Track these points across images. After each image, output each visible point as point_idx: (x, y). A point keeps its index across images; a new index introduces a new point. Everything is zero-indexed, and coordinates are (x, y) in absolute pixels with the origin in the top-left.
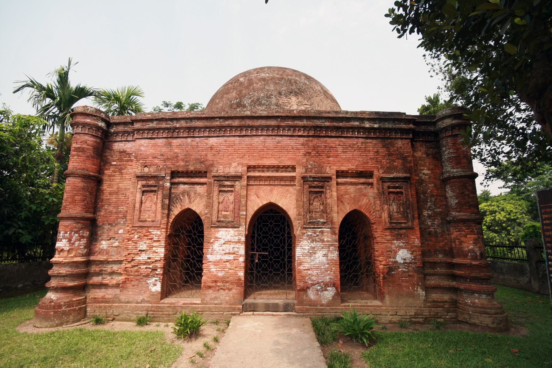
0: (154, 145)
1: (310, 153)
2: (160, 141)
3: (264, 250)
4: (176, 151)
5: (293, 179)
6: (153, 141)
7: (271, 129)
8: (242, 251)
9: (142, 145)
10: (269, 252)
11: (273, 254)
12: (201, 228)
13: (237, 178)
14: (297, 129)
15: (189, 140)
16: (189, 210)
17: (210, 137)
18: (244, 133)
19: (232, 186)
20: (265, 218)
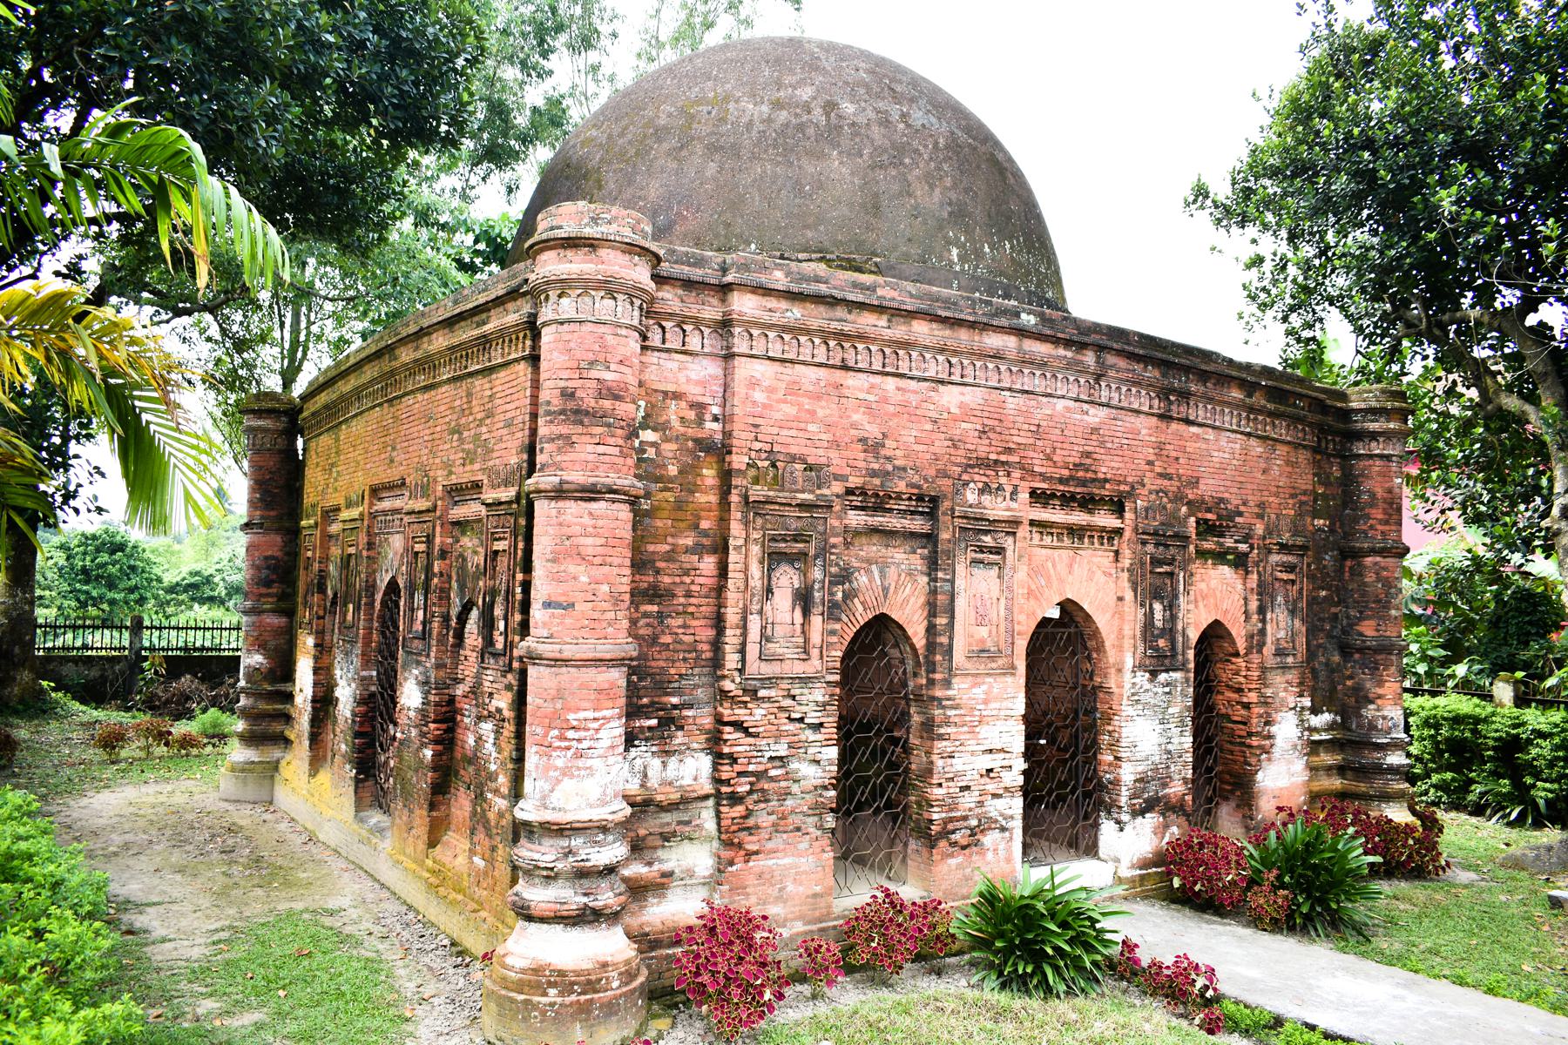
4: (856, 417)
5: (1118, 532)
6: (788, 370)
8: (1018, 744)
9: (753, 384)
15: (891, 383)
16: (883, 615)
17: (942, 382)
18: (1026, 382)
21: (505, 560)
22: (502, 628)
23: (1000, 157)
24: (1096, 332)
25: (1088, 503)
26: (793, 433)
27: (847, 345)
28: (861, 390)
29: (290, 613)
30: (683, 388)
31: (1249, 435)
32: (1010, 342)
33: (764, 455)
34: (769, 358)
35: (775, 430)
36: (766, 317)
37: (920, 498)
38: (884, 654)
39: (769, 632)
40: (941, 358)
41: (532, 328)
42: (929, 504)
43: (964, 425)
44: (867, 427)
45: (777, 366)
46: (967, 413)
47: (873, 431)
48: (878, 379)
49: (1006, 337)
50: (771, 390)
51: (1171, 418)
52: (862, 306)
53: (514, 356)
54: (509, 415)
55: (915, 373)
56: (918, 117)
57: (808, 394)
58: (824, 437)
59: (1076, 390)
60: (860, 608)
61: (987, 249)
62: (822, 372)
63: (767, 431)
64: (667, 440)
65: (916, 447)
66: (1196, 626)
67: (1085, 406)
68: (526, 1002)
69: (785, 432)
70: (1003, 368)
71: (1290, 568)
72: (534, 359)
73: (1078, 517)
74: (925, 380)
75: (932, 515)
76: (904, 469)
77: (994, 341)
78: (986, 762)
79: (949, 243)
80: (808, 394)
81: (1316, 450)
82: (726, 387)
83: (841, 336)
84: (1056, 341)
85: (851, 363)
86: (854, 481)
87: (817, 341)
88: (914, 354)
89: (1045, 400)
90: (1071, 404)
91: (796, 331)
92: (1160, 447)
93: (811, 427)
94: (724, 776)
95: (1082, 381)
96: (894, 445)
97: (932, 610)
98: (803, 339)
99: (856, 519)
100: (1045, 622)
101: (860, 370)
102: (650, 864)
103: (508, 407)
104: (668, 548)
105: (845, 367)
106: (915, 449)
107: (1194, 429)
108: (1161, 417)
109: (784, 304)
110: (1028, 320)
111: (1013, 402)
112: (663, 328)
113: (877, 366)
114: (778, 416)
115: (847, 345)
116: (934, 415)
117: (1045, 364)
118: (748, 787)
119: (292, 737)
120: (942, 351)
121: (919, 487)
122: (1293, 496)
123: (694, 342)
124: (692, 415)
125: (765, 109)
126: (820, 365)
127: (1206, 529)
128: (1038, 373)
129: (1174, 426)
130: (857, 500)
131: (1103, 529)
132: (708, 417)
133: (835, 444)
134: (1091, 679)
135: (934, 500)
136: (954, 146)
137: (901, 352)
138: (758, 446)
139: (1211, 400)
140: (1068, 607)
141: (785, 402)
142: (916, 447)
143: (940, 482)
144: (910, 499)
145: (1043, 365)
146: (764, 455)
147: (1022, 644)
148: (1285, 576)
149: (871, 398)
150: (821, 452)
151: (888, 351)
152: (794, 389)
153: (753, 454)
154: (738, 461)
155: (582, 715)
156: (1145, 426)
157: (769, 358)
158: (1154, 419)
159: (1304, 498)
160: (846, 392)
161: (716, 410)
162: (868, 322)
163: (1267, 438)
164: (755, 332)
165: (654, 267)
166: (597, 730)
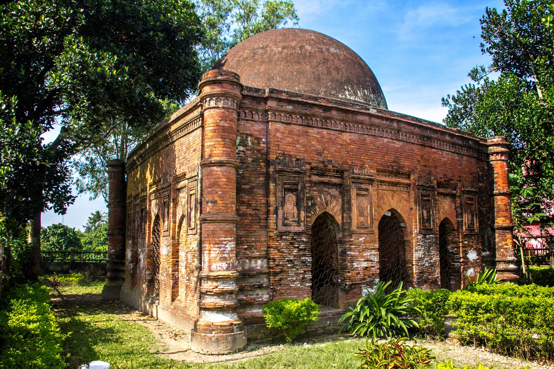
2: (297, 128)
4: (313, 143)
8: (376, 259)
9: (277, 130)
15: (325, 132)
19: (367, 190)
21: (194, 197)
22: (194, 221)
23: (362, 63)
24: (397, 116)
25: (397, 174)
26: (291, 148)
27: (309, 118)
28: (314, 134)
29: (124, 235)
30: (253, 132)
31: (453, 152)
32: (366, 118)
33: (281, 155)
34: (282, 122)
35: (285, 147)
36: (280, 108)
37: (337, 171)
38: (327, 227)
39: (285, 216)
40: (342, 123)
41: (202, 115)
42: (340, 173)
43: (351, 146)
44: (318, 146)
45: (285, 125)
46: (353, 142)
47: (319, 147)
48: (320, 130)
50: (283, 133)
51: (425, 146)
52: (314, 105)
53: (196, 127)
54: (194, 148)
55: (333, 128)
56: (332, 50)
57: (296, 135)
58: (302, 149)
59: (391, 135)
60: (318, 209)
62: (301, 128)
63: (282, 147)
64: (247, 150)
65: (335, 153)
66: (439, 219)
67: (395, 141)
68: (205, 336)
69: (289, 147)
70: (364, 127)
71: (471, 199)
72: (203, 127)
73: (394, 179)
74: (337, 131)
75: (342, 177)
76: (331, 161)
77: (360, 118)
78: (365, 264)
79: (345, 90)
80: (296, 135)
81: (478, 159)
82: (267, 132)
83: (306, 115)
84: (382, 118)
85: (311, 124)
86: (314, 165)
87: (298, 117)
88: (333, 122)
89: (380, 138)
90: (390, 140)
91: (291, 113)
92: (422, 156)
93: (298, 146)
94: (271, 266)
95: (393, 132)
96: (327, 152)
97: (343, 210)
98: (293, 116)
99: (315, 178)
100: (384, 217)
101: (314, 127)
102: (246, 296)
103: (194, 145)
104: (249, 187)
105: (309, 126)
106: (334, 155)
107: (434, 150)
108: (421, 145)
109: (286, 104)
110: (373, 111)
112: (245, 113)
113: (320, 126)
114: (286, 142)
115: (309, 118)
116: (341, 142)
117: (379, 126)
118: (280, 270)
119: (125, 277)
120: (342, 121)
121: (337, 167)
122: (471, 174)
123: (256, 117)
124: (256, 141)
125: (280, 49)
126: (300, 125)
127: (440, 185)
128: (377, 129)
129: (427, 149)
130: (315, 172)
131: (404, 184)
132: (261, 142)
133: (306, 151)
134: (403, 238)
136: (346, 58)
137: (328, 121)
138: (279, 152)
139: (439, 140)
140: (392, 210)
141: (288, 137)
142: (335, 153)
143: (344, 165)
144: (334, 172)
145: (378, 126)
146: (281, 155)
147: (376, 224)
148: (469, 202)
149: (318, 136)
150: (301, 154)
151: (323, 120)
152: (291, 132)
153: (277, 155)
154: (273, 157)
155: (221, 239)
156: (416, 148)
157: (282, 122)
158: (419, 146)
159: (474, 175)
160: (309, 134)
161: (264, 140)
162: (317, 110)
163: (460, 154)
164: (277, 114)
165: (241, 91)
166: (226, 245)
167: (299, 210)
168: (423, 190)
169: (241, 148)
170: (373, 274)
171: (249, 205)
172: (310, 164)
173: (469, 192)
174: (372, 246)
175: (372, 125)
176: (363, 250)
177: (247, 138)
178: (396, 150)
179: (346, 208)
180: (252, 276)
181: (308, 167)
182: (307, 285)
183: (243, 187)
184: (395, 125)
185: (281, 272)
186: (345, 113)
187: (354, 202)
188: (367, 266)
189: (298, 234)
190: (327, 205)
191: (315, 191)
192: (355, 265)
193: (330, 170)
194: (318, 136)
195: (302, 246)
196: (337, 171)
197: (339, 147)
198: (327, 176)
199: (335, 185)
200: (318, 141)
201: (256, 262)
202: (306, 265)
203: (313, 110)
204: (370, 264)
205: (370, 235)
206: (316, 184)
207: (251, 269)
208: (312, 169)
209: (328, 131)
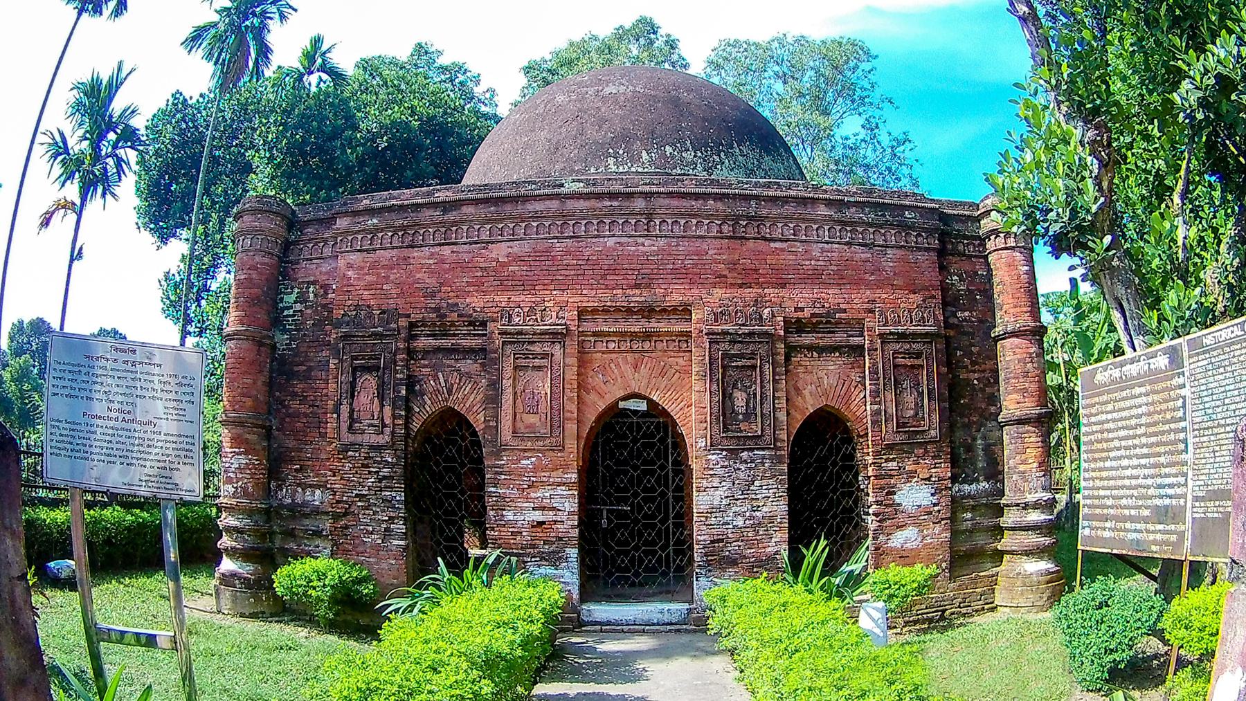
0: (374, 265)
1: (725, 276)
2: (388, 254)
3: (620, 501)
4: (418, 276)
7: (633, 222)
10: (632, 505)
11: (640, 508)
12: (475, 452)
13: (557, 337)
14: (694, 221)
15: (447, 250)
17: (492, 243)
19: (544, 356)
20: (621, 428)
47: (432, 282)
48: (437, 249)
49: (547, 202)
60: (429, 402)
61: (644, 154)
67: (640, 240)
78: (538, 516)
84: (599, 196)
91: (374, 231)
107: (772, 245)
110: (571, 187)
111: (559, 246)
129: (751, 244)
135: (484, 324)
145: (583, 215)
149: (431, 261)
150: (392, 301)
167: (382, 406)
168: (733, 342)
169: (298, 307)
170: (560, 539)
171: (304, 400)
172: (408, 316)
173: (902, 336)
174: (556, 476)
175: (565, 216)
176: (529, 487)
177: (308, 288)
178: (646, 259)
179: (493, 399)
180: (306, 516)
181: (403, 323)
182: (396, 542)
183: (296, 369)
184: (639, 204)
185: (345, 514)
186: (496, 205)
187: (507, 383)
188: (541, 519)
189: (378, 448)
190: (450, 391)
191: (426, 366)
192: (509, 515)
193: (453, 324)
194: (431, 261)
195: (385, 472)
196: (471, 324)
197: (480, 274)
198: (454, 335)
199: (470, 352)
200: (430, 271)
201: (313, 494)
202: (393, 507)
203: (420, 215)
204: (548, 516)
205: (551, 453)
206: (426, 353)
207: (305, 504)
208: (412, 326)
209: (455, 248)
